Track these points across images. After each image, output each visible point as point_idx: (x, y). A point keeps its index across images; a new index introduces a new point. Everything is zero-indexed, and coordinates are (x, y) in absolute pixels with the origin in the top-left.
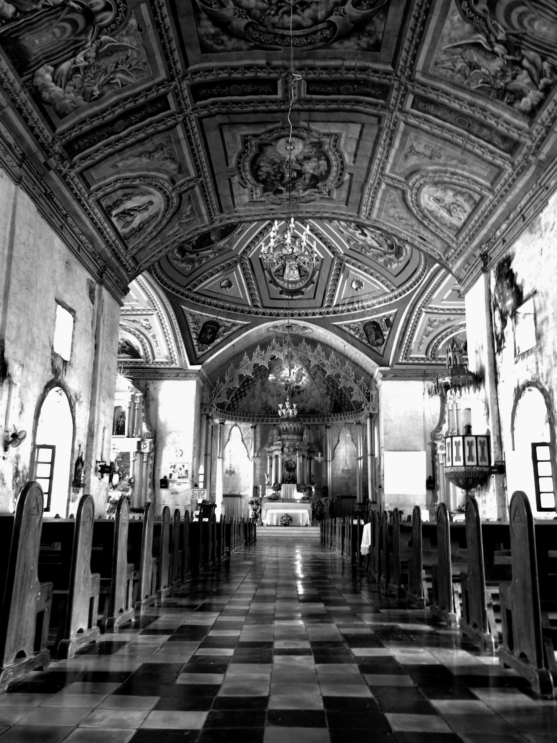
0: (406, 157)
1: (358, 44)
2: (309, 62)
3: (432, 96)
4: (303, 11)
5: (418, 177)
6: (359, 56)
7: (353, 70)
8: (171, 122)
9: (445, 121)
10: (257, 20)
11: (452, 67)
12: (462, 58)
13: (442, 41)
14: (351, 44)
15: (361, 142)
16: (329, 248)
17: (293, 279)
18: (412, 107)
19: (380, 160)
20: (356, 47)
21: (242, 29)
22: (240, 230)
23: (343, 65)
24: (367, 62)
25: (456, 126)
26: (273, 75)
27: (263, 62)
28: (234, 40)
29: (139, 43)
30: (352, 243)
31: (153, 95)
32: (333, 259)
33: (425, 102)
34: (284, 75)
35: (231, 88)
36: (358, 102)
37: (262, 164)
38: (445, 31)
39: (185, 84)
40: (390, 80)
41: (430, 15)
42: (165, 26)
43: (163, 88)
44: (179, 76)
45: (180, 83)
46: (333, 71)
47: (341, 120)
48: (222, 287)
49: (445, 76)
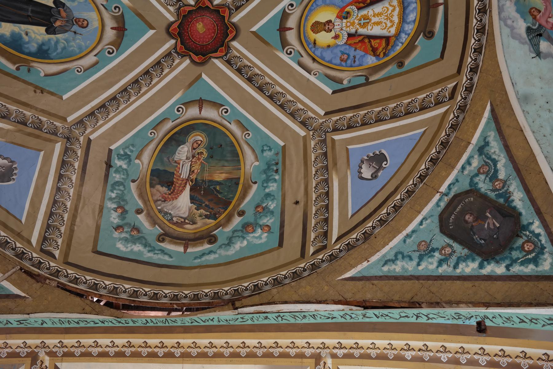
17: (397, 9)
22: (234, 127)
48: (374, 176)
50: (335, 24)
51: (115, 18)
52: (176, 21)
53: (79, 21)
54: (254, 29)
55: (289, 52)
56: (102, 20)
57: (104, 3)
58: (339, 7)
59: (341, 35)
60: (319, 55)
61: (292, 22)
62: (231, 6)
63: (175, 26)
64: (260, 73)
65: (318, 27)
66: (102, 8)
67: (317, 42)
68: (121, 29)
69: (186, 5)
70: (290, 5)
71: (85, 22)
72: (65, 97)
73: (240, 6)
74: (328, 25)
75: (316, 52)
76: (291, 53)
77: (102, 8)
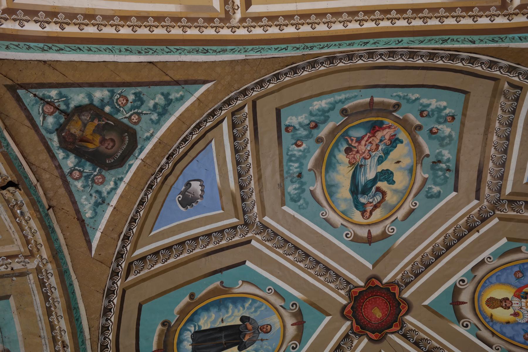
16: (471, 229)
30: (436, 189)
32: (501, 219)
50: (513, 302)
51: (294, 315)
52: (349, 303)
53: (264, 328)
54: (426, 303)
55: (465, 325)
56: (283, 321)
57: (282, 304)
58: (516, 286)
59: (521, 313)
60: (499, 330)
61: (465, 297)
62: (400, 283)
63: (349, 308)
64: (438, 346)
65: (493, 303)
66: (281, 309)
67: (493, 317)
68: (300, 324)
69: (356, 287)
70: (461, 280)
71: (269, 327)
73: (410, 282)
74: (505, 302)
75: (495, 327)
76: (467, 326)
77: (281, 309)
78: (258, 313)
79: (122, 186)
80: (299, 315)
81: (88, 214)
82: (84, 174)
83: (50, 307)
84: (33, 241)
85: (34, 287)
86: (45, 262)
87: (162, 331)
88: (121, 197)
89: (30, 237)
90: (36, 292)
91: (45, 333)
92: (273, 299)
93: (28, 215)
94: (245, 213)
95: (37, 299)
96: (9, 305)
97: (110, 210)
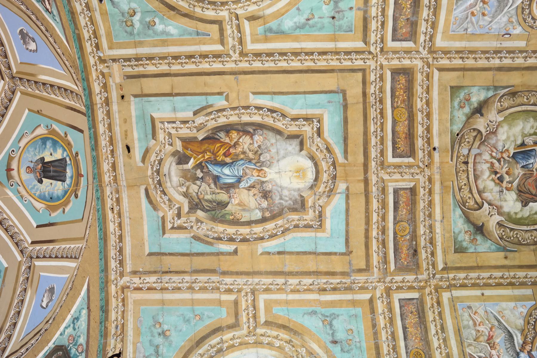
0: (314, 313)
1: (460, 232)
2: (437, 187)
3: (430, 316)
4: (493, 180)
5: (284, 335)
6: (447, 235)
7: (431, 232)
8: (373, 38)
9: (405, 338)
10: (485, 141)
11: (478, 324)
12: (491, 329)
13: (494, 304)
14: (459, 224)
15: (312, 257)
18: (399, 300)
19: (285, 284)
20: (457, 231)
21: (475, 127)
23: (436, 221)
24: (442, 244)
25: (407, 353)
26: (420, 154)
27: (436, 144)
28: (464, 118)
29: (493, 30)
31: (423, 27)
33: (418, 311)
34: (421, 164)
35: (404, 110)
36: (384, 244)
37: (256, 137)
38: (504, 304)
39: (419, 63)
40: (428, 269)
41: (510, 287)
42: (493, 58)
43: (425, 41)
44: (430, 60)
45: (421, 58)
46: (427, 213)
47: (351, 228)
49: (462, 321)
57: (19, 187)
71: (28, 171)
72: (27, 111)
78: (33, 184)
79: (62, 329)
80: (9, 177)
81: (84, 312)
82: (76, 347)
83: (119, 243)
84: (120, 300)
85: (128, 262)
86: (115, 281)
87: (78, 191)
88: (64, 320)
89: (121, 304)
90: (128, 256)
91: (126, 221)
92: (24, 192)
93: (113, 326)
94: (30, 268)
95: (128, 251)
96: (150, 248)
97: (72, 312)
